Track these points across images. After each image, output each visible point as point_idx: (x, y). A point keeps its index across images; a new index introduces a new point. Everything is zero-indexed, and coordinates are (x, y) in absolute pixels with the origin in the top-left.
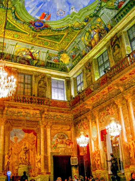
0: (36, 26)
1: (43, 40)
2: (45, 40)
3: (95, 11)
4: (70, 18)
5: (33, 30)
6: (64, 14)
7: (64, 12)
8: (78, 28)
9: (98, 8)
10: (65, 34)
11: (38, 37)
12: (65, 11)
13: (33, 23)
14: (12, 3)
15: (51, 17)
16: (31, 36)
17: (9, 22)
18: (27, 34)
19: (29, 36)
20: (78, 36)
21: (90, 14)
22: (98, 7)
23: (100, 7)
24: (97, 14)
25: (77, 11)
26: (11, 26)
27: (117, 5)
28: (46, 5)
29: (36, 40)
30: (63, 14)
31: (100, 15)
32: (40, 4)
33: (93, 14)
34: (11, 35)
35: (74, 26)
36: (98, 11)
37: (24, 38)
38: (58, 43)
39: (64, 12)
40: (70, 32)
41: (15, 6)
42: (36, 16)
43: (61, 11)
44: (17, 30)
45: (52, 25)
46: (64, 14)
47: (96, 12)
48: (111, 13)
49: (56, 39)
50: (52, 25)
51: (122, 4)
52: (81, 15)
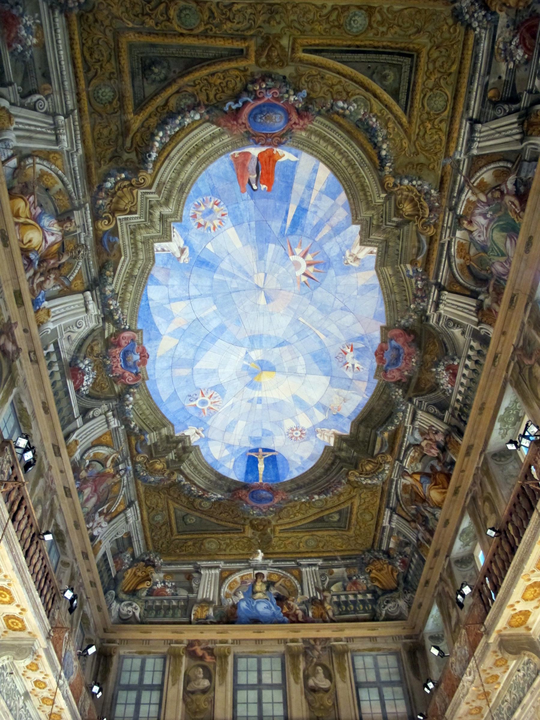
0: (275, 106)
1: (215, 37)
2: (205, 35)
3: (113, 291)
4: (166, 211)
5: (284, 77)
6: (195, 216)
7: (200, 225)
8: (109, 185)
9: (112, 308)
10: (136, 122)
11: (248, 48)
12: (201, 229)
13: (294, 117)
14: (397, 210)
15: (232, 175)
16: (285, 42)
17: (398, 101)
18: (305, 51)
19: (295, 40)
20: (81, 152)
21: (115, 271)
22: (116, 310)
23: (111, 313)
24: (100, 291)
25: (163, 250)
26: (385, 77)
27: (82, 366)
28: (276, 225)
29: (250, 28)
30: (199, 214)
31: (90, 298)
32: (296, 223)
33: (110, 280)
34: (381, 23)
35: (126, 183)
36: (104, 305)
37: (317, 17)
38: (132, 37)
39: (202, 221)
40: (123, 144)
41: (383, 195)
42: (293, 158)
43: (211, 221)
44: (357, 57)
45: (213, 137)
46: (195, 216)
47: (108, 293)
48: (74, 336)
49: (154, 63)
50: (213, 137)
51: (74, 383)
52: (140, 245)
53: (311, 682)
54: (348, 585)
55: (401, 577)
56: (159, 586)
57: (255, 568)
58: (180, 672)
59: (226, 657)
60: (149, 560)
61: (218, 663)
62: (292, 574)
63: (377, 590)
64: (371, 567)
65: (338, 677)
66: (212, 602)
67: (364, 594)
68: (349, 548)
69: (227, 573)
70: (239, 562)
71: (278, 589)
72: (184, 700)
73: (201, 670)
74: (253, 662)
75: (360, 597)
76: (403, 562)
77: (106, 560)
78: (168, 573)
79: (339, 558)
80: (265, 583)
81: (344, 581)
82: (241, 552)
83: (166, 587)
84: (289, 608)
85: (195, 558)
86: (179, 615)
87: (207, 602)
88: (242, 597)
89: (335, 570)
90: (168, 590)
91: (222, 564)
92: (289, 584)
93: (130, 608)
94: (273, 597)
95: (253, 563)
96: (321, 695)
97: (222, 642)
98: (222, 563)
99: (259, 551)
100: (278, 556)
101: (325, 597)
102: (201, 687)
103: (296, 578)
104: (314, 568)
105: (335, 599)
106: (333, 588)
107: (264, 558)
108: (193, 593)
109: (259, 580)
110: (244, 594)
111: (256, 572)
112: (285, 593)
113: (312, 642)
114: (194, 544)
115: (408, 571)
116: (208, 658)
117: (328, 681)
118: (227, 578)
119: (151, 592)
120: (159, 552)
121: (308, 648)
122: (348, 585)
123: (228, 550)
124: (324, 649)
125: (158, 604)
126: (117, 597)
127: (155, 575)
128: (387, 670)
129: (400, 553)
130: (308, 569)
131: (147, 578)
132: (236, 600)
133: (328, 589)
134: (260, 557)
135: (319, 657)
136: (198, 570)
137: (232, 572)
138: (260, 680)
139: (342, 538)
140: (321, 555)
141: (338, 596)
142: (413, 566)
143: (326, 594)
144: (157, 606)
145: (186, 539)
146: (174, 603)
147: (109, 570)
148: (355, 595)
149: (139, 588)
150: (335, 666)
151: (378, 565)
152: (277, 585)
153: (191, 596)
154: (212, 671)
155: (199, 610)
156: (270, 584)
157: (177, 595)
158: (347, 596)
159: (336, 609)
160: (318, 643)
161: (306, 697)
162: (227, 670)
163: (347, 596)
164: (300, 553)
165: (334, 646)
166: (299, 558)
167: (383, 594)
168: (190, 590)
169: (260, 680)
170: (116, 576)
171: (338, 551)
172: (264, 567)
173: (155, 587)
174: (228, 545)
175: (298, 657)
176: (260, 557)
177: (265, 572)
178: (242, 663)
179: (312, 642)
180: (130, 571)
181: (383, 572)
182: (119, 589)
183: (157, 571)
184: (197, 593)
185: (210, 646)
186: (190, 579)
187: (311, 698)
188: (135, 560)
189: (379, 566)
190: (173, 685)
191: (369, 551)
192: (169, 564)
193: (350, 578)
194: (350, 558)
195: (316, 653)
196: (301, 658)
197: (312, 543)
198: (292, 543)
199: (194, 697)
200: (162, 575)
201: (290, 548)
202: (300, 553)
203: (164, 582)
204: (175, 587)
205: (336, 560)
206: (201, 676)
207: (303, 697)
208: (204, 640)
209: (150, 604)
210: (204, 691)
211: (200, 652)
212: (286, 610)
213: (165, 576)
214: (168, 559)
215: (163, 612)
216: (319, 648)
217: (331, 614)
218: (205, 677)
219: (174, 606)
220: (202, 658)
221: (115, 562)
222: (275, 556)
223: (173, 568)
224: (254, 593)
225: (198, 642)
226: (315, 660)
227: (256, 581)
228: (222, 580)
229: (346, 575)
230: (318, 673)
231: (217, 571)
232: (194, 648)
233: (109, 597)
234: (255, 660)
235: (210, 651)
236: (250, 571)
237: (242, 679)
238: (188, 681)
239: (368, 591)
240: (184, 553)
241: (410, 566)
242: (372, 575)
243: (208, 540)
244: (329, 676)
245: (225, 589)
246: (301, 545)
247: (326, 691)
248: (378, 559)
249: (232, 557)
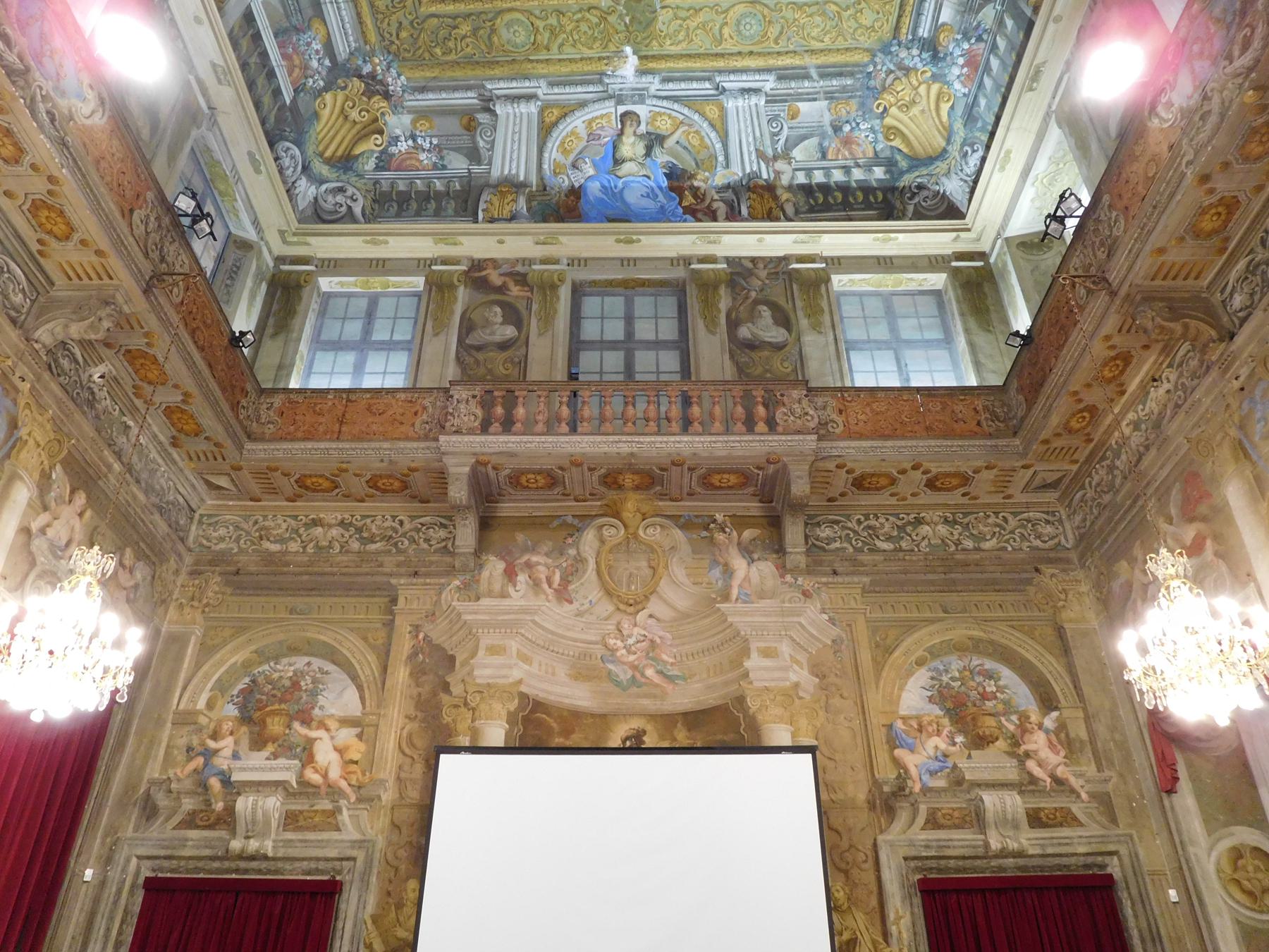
53: (744, 332)
54: (833, 145)
55: (959, 111)
56: (403, 146)
57: (620, 100)
58: (452, 312)
59: (554, 287)
60: (372, 76)
61: (537, 298)
62: (702, 115)
63: (898, 157)
64: (888, 98)
65: (804, 322)
66: (523, 185)
67: (868, 168)
68: (841, 44)
69: (556, 112)
70: (582, 83)
71: (672, 153)
72: (458, 359)
73: (498, 310)
74: (615, 304)
75: (858, 174)
76: (971, 62)
77: (257, 37)
78: (422, 114)
79: (813, 73)
80: (641, 137)
81: (823, 136)
82: (587, 53)
83: (417, 147)
84: (695, 196)
85: (479, 72)
86: (450, 212)
87: (512, 186)
88: (591, 172)
89: (803, 106)
90: (423, 156)
91: (542, 89)
92: (696, 142)
93: (340, 198)
94: (661, 171)
95: (614, 86)
96: (766, 353)
97: (545, 261)
98: (543, 83)
99: (628, 50)
100: (671, 65)
101: (778, 173)
102: (497, 338)
103: (712, 125)
104: (754, 99)
105: (801, 178)
106: (797, 153)
107: (641, 72)
108: (479, 163)
109: (629, 130)
110: (595, 165)
111: (622, 109)
112: (689, 164)
113: (750, 265)
114: (475, 31)
115: (981, 85)
116: (515, 290)
117: (783, 331)
118: (555, 124)
119: (384, 161)
120: (396, 56)
121: (738, 274)
122: (833, 145)
123: (555, 48)
124: (774, 275)
125: (402, 186)
126: (305, 168)
127: (391, 120)
128: (914, 321)
129: (966, 37)
130: (740, 102)
131: (374, 127)
132: (577, 179)
133: (786, 156)
134: (629, 66)
135: (762, 290)
136: (487, 104)
137: (567, 110)
138: (630, 334)
139: (824, 14)
140: (772, 62)
141: (809, 171)
142: (995, 63)
143: (780, 165)
144: (400, 193)
145: (455, 17)
146: (439, 185)
147: (271, 75)
148: (847, 170)
149: (357, 151)
150: (799, 304)
151: (903, 89)
152: (670, 143)
153: (476, 169)
154: (524, 312)
155: (496, 201)
156: (653, 141)
157: (444, 167)
158: (827, 170)
159: (801, 199)
160: (761, 265)
161: (732, 357)
162: (556, 311)
163: (827, 170)
164: (722, 55)
165: (797, 270)
166: (720, 72)
167: (910, 169)
168: (474, 155)
169: (630, 334)
170: (294, 100)
171: (813, 52)
172: (640, 96)
173: (393, 149)
174: (553, 33)
175: (716, 288)
176: (629, 66)
177: (642, 110)
178: (591, 305)
179: (750, 265)
180: (328, 97)
181: (915, 111)
182: (310, 149)
183: (396, 108)
184: (490, 164)
185: (519, 268)
186: (472, 125)
187: (743, 359)
188: (339, 72)
189: (906, 95)
190: (436, 335)
191: (885, 49)
192: (423, 90)
193: (837, 129)
194: (840, 75)
195: (757, 283)
196: (723, 290)
197: (752, 28)
198: (703, 26)
199: (480, 356)
200: (407, 119)
201: (702, 43)
202: (722, 55)
203: (413, 137)
204: (438, 149)
205: (807, 77)
206: (500, 320)
207: (727, 356)
208: (507, 261)
209: (385, 186)
210: (504, 346)
211: (495, 278)
212: (689, 200)
213: (414, 122)
214: (421, 75)
215: (414, 205)
216: (763, 274)
217: (790, 210)
218: (506, 321)
219: (437, 193)
220: (502, 289)
221: (285, 56)
222: (662, 65)
223: (431, 99)
224: (618, 162)
225: (494, 263)
226: (753, 294)
227: (621, 133)
228: (546, 130)
229: (827, 118)
230: (761, 316)
231: (533, 108)
232: (484, 273)
233: (286, 162)
234: (622, 299)
235: (521, 279)
236: (608, 108)
237: (590, 330)
238: (467, 326)
239: (877, 160)
240: (452, 57)
241: (987, 69)
242: (888, 121)
243: (507, 17)
244: (784, 320)
245: (553, 153)
246: (726, 31)
247: (779, 347)
248: (907, 71)
249: (565, 69)
